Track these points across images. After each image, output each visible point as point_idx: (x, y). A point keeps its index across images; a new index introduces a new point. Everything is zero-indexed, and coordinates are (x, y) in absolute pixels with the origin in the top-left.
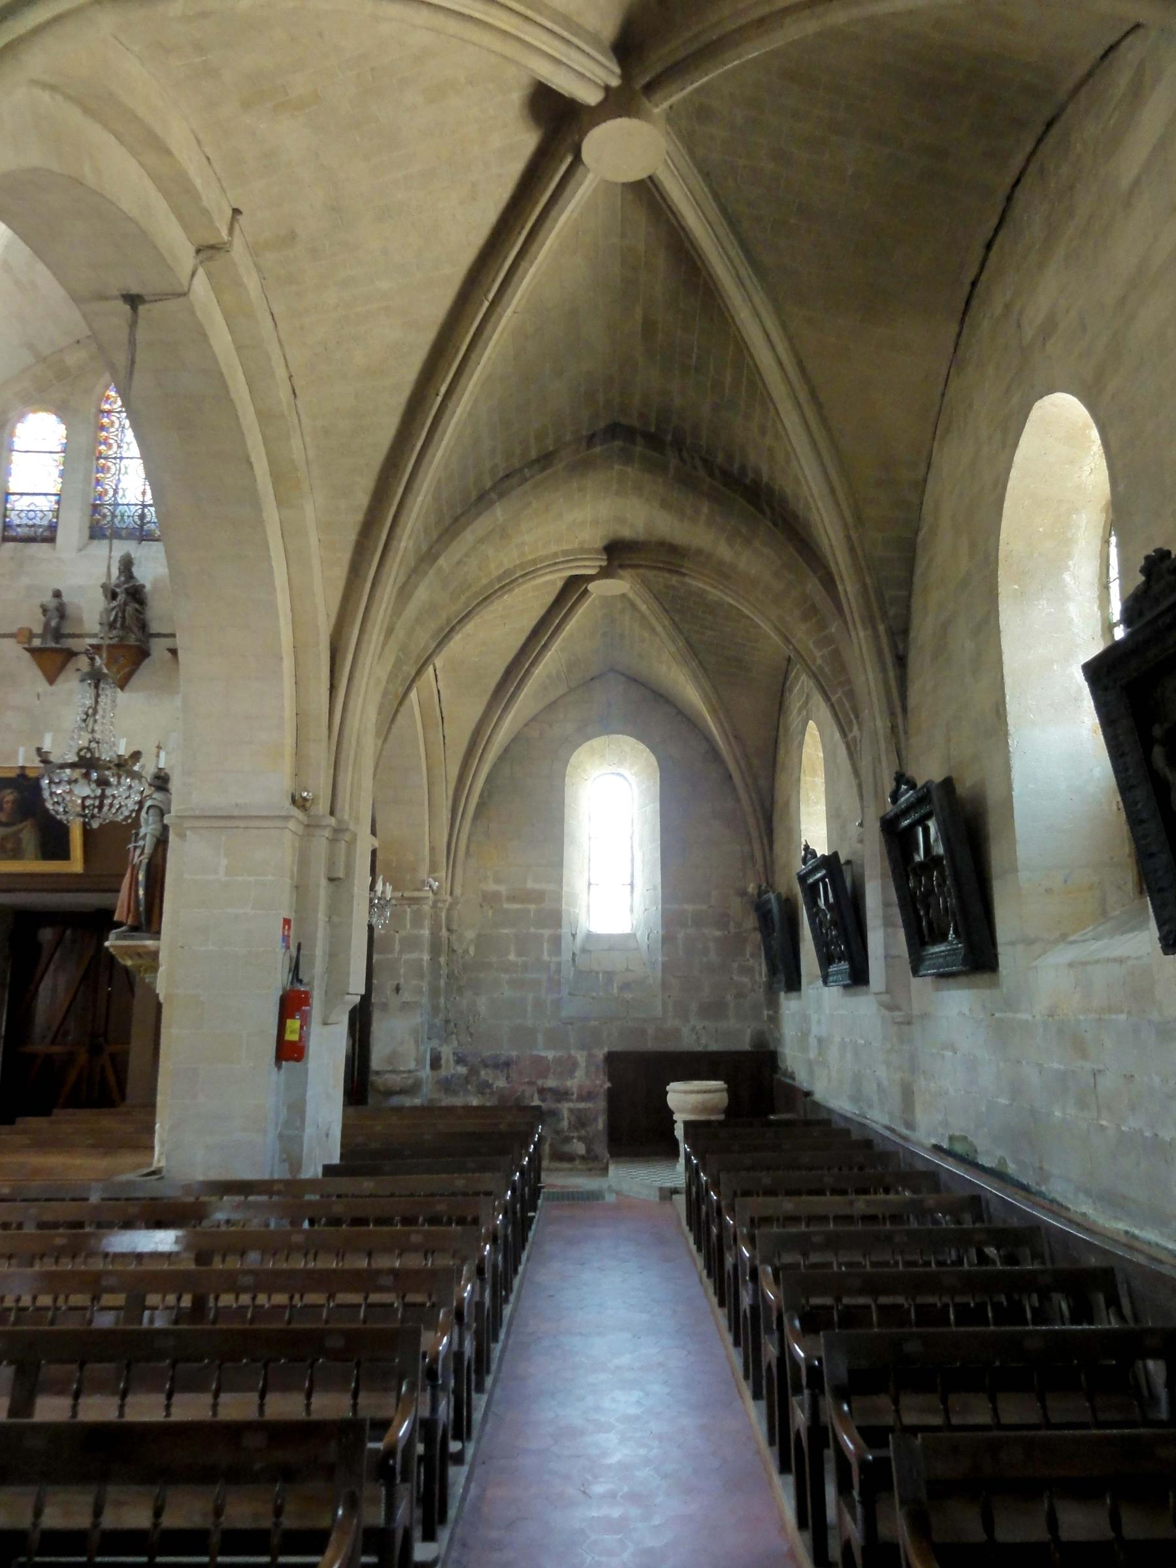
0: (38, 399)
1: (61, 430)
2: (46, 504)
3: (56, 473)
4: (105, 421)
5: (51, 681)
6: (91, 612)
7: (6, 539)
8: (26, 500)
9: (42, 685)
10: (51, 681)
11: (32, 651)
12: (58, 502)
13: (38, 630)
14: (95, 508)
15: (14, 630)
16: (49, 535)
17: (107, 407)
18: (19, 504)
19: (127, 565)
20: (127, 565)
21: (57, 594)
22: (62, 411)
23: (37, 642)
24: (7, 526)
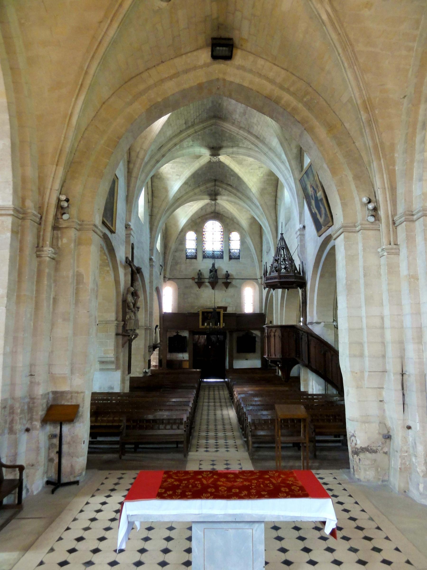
0: (190, 230)
1: (196, 235)
2: (194, 251)
3: (195, 245)
4: (204, 233)
5: (199, 287)
6: (206, 274)
7: (187, 258)
8: (190, 250)
9: (198, 289)
10: (199, 287)
11: (196, 283)
12: (196, 251)
13: (197, 277)
14: (204, 252)
15: (191, 277)
16: (195, 257)
17: (204, 230)
18: (189, 251)
19: (213, 265)
20: (213, 265)
21: (200, 271)
22: (196, 232)
23: (196, 280)
24: (187, 256)
